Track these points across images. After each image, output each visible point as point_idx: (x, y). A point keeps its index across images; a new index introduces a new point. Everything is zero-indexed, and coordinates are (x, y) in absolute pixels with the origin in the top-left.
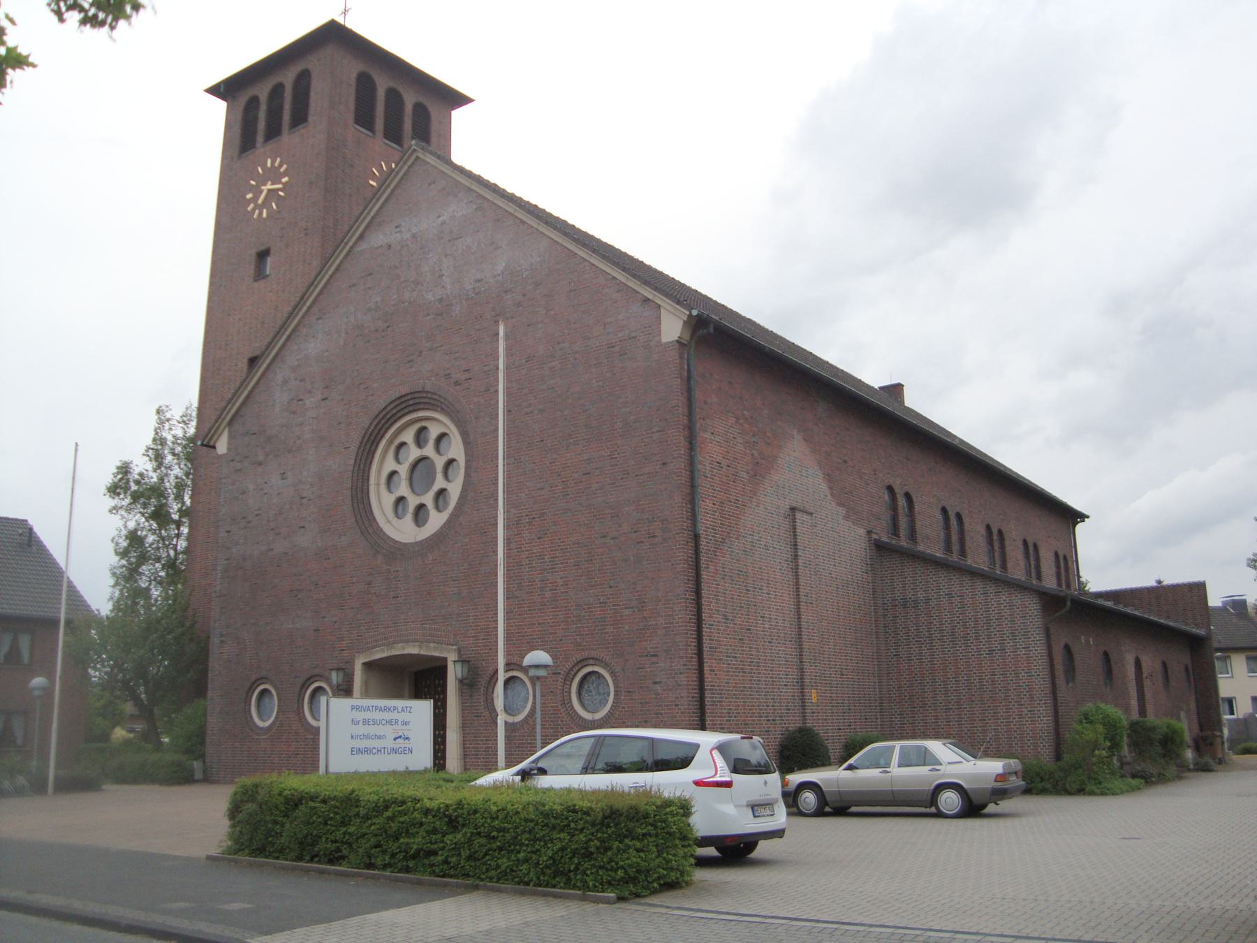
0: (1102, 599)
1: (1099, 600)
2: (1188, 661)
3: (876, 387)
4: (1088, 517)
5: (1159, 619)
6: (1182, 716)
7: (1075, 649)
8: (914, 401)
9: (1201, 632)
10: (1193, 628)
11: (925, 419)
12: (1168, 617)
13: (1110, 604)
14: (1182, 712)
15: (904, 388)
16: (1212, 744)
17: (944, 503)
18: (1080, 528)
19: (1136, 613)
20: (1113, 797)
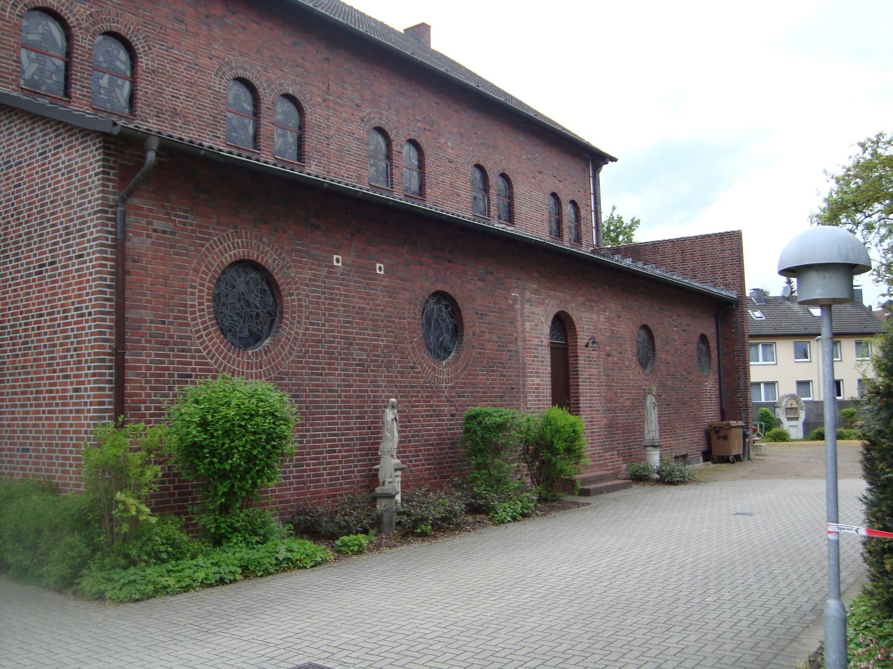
0: (620, 256)
1: (616, 257)
2: (711, 333)
3: (401, 30)
4: (614, 160)
5: (684, 278)
6: (648, 402)
7: (657, 331)
8: (440, 42)
9: (733, 294)
10: (723, 289)
11: (486, 82)
12: (694, 277)
13: (627, 262)
14: (649, 397)
15: (431, 29)
16: (726, 438)
17: (376, 123)
18: (606, 171)
19: (658, 272)
20: (417, 548)
